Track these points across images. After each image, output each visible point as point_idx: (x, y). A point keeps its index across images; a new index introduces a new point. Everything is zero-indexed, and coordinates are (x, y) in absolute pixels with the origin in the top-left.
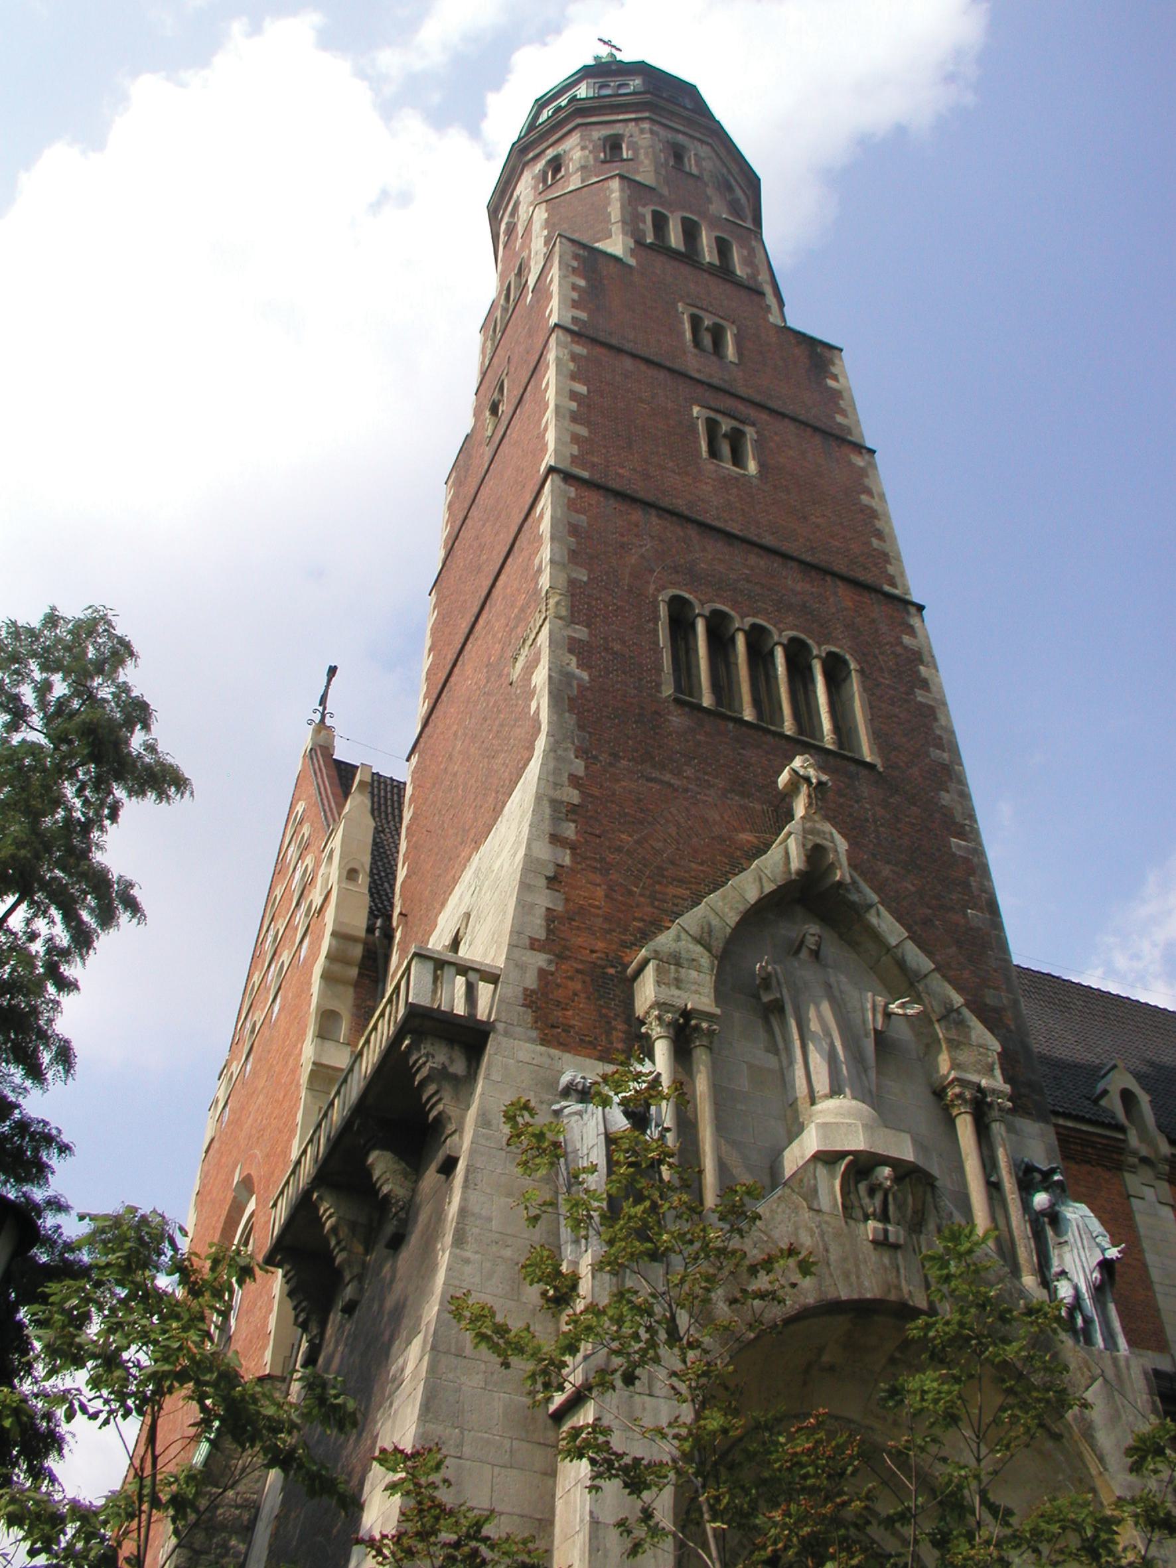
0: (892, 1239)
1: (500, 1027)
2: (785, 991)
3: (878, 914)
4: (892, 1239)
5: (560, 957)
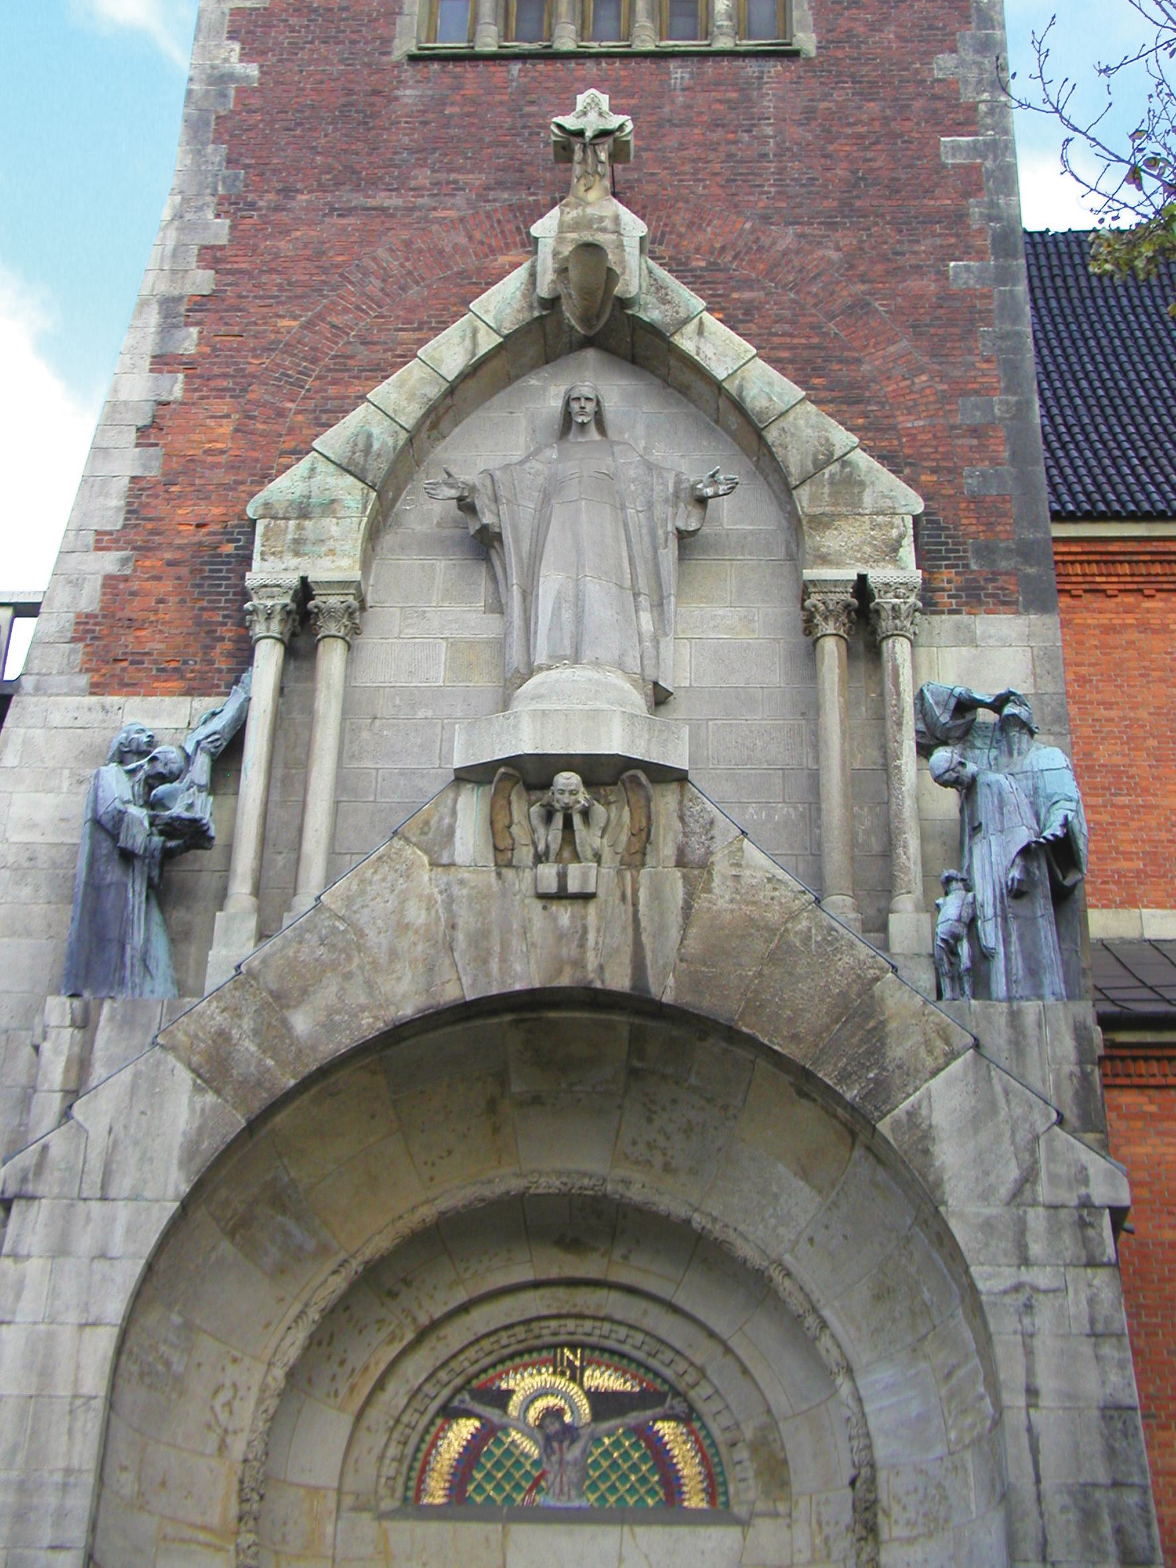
1: (28, 683)
3: (700, 331)
4: (573, 887)
5: (145, 549)
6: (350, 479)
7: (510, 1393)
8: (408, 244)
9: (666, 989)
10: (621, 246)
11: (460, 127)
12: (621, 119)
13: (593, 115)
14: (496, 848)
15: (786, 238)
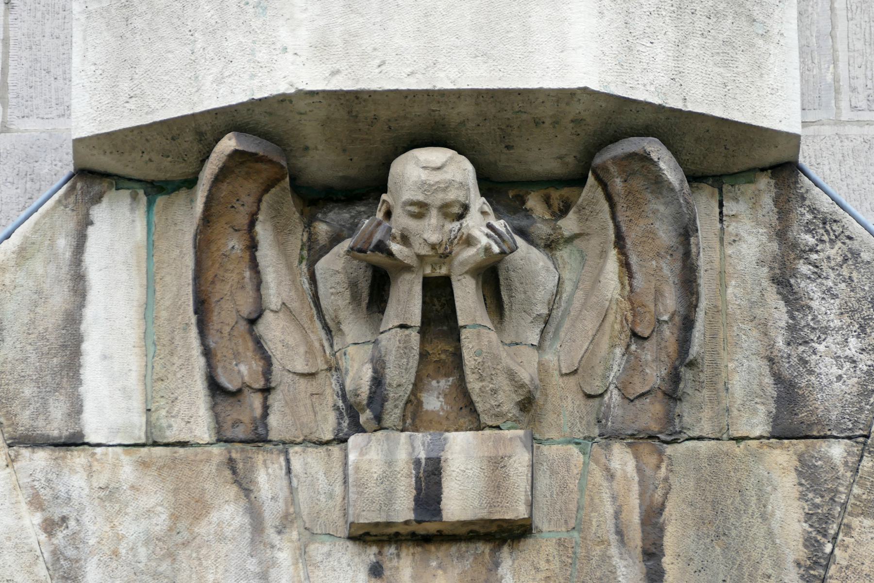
14: (215, 387)
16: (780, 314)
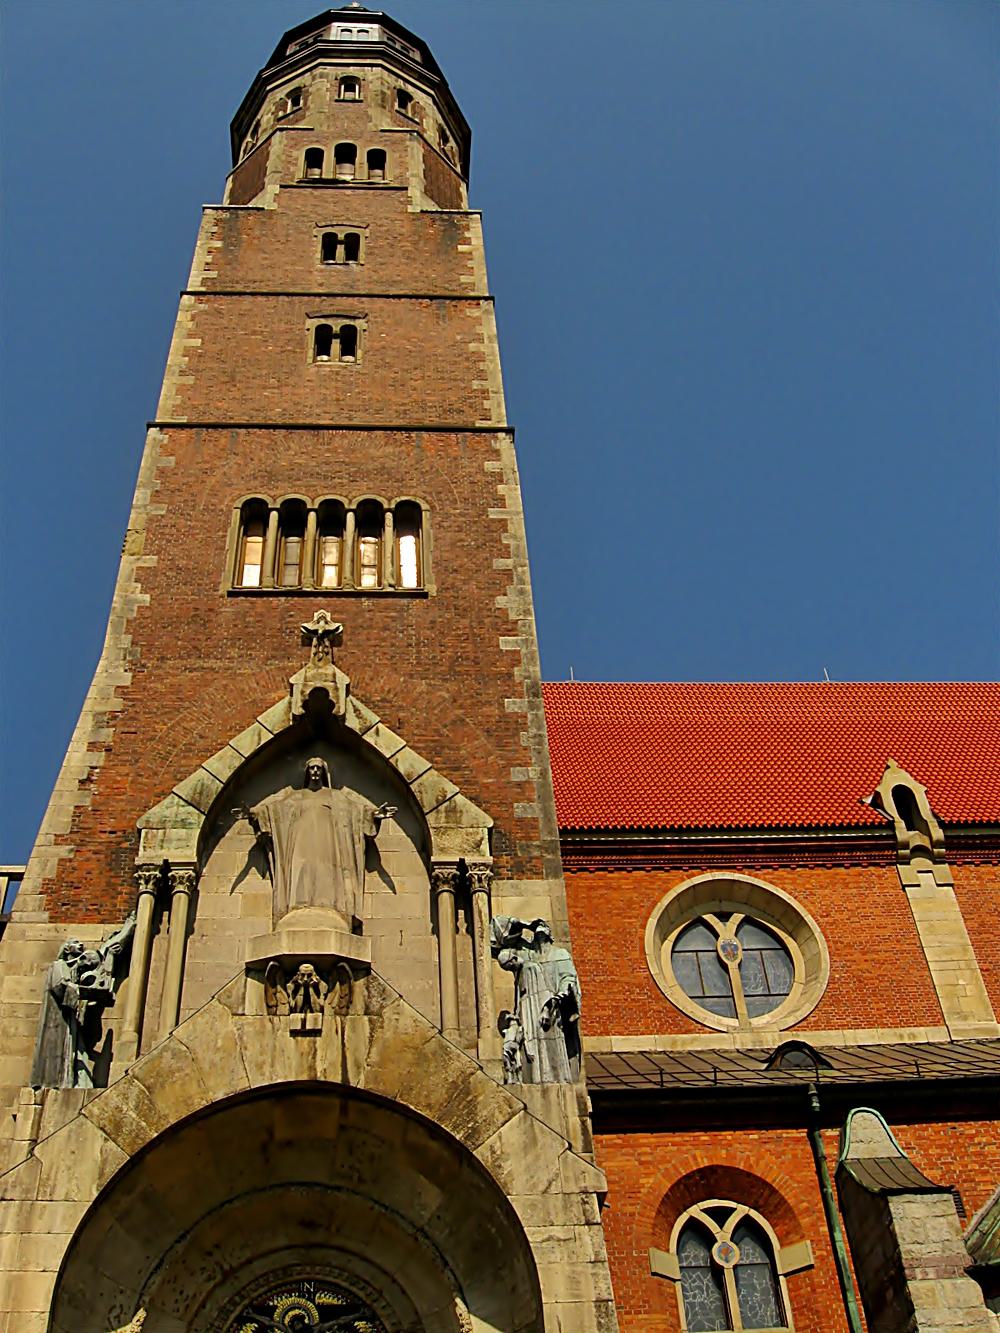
0: (309, 1027)
2: (273, 824)
3: (377, 732)
4: (309, 1027)
6: (191, 809)
7: (276, 1307)
8: (225, 686)
9: (359, 1081)
10: (337, 689)
11: (253, 627)
12: (337, 625)
13: (322, 623)
15: (422, 686)
16: (366, 993)
